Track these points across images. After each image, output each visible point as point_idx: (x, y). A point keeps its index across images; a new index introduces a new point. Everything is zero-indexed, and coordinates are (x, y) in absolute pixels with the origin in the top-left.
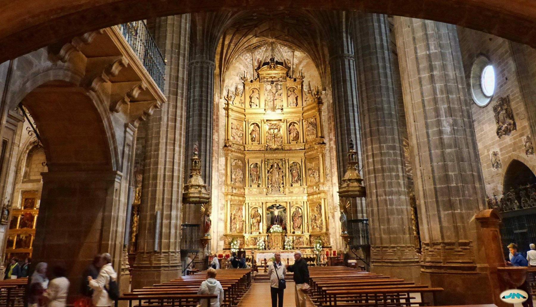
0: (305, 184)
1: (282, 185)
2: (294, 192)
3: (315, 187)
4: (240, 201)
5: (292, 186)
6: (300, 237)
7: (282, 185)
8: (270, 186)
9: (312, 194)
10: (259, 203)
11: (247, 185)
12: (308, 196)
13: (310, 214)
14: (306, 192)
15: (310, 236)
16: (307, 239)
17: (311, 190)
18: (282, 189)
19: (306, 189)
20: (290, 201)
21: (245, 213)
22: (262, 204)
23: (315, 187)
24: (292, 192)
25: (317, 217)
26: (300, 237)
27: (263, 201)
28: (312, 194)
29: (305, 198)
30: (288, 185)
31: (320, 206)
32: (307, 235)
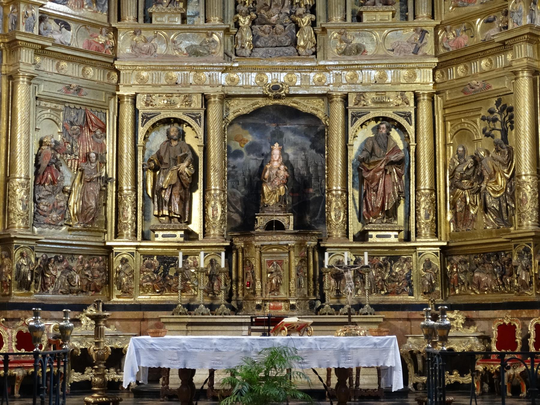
0: (424, 12)
1: (307, 18)
2: (370, 49)
3: (479, 23)
4: (96, 88)
5: (358, 18)
6: (395, 259)
7: (307, 18)
8: (244, 21)
9: (465, 56)
10: (188, 98)
11: (129, 17)
12: (444, 65)
13: (448, 155)
14: (429, 47)
15: (445, 252)
16: (428, 264)
17: (453, 39)
18: (305, 38)
19: (430, 38)
20: (344, 89)
21: (119, 150)
22: (206, 100)
23: (479, 23)
24: (359, 50)
25: (488, 164)
26: (393, 256)
27: (207, 90)
28: (465, 56)
29: (424, 80)
30: (337, 19)
31: (509, 112)
32: (428, 246)
